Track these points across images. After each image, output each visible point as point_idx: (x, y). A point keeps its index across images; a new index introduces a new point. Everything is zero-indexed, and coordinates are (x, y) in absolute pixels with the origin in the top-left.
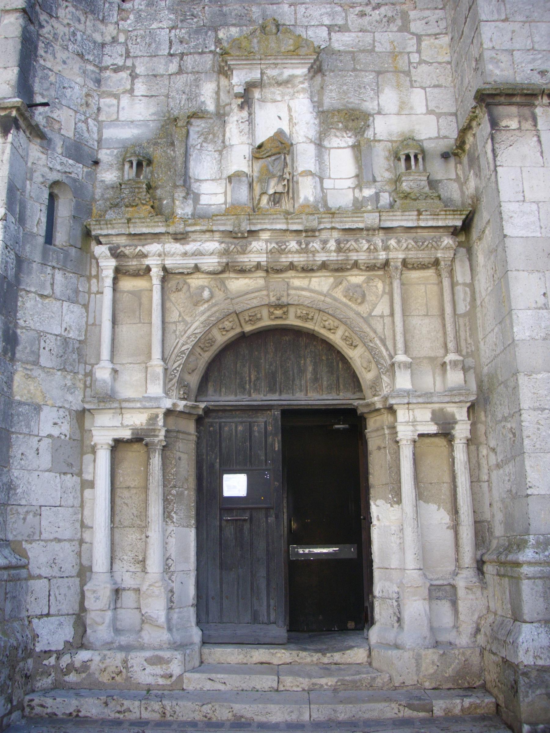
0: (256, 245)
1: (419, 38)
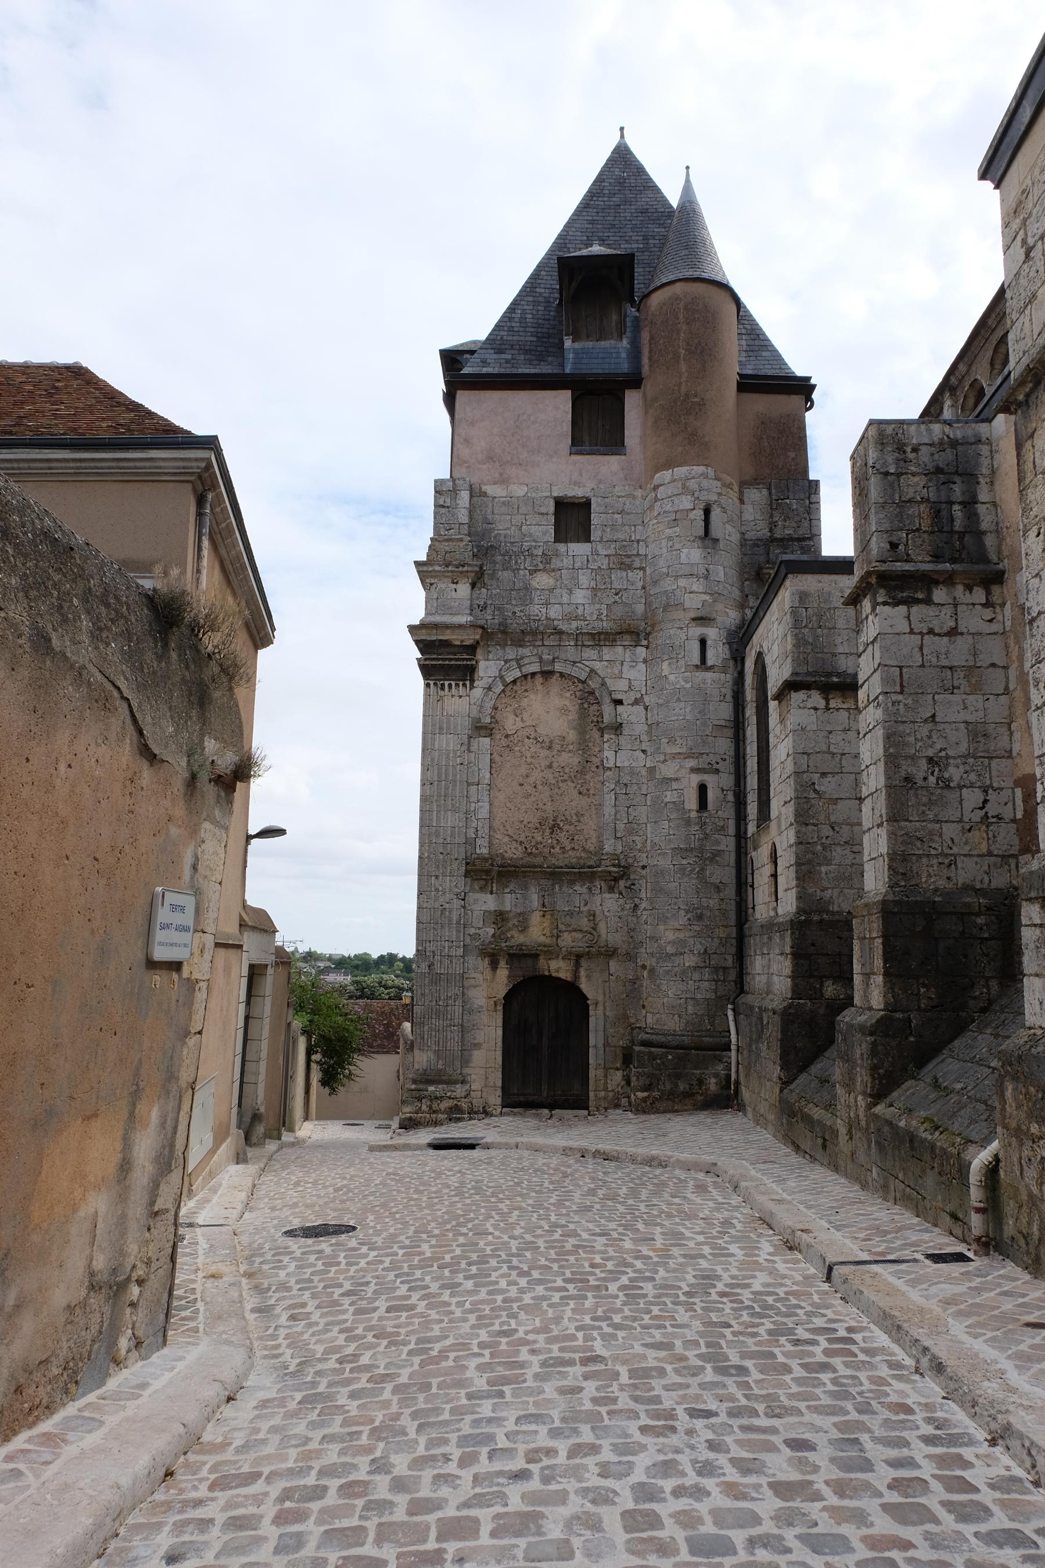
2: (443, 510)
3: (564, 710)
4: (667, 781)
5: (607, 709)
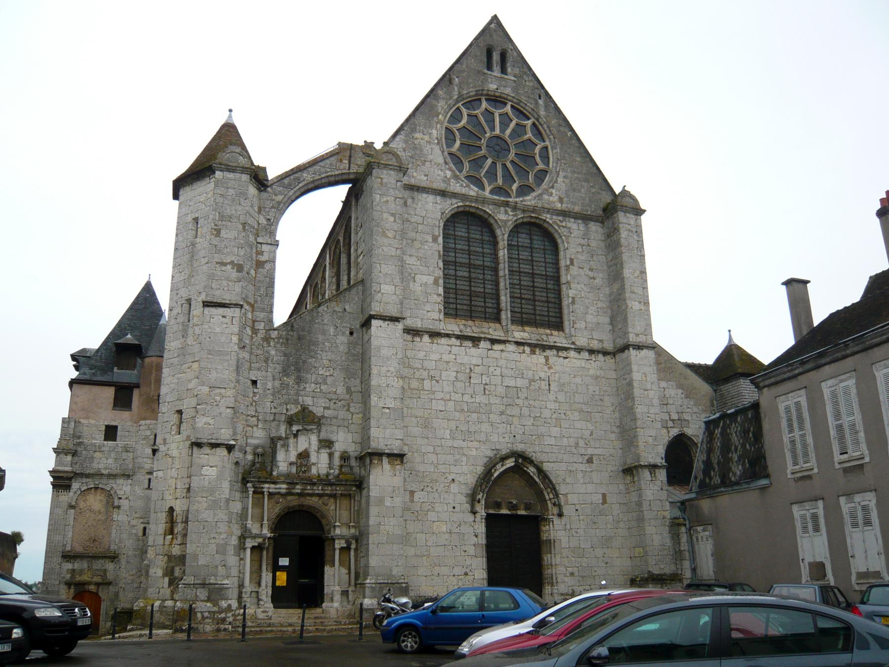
0: (298, 487)
1: (353, 414)
3: (101, 500)
4: (133, 526)
5: (116, 501)
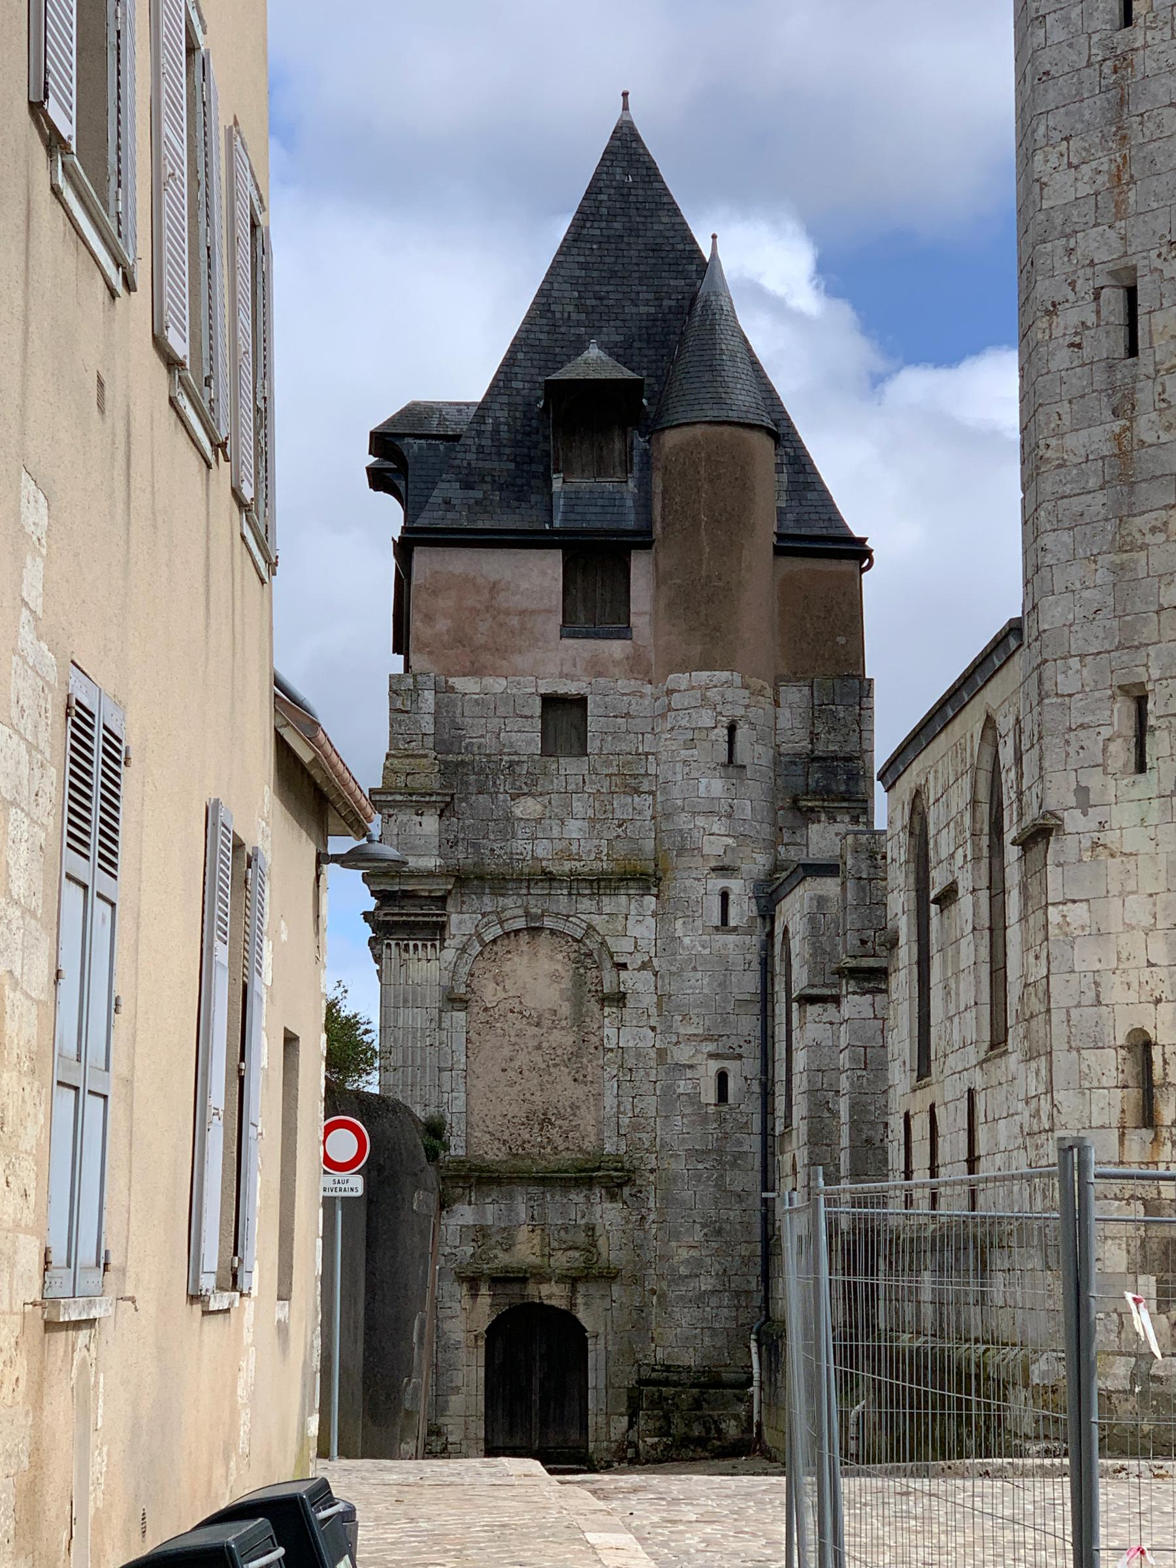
2: (401, 717)
3: (555, 977)
5: (608, 976)
